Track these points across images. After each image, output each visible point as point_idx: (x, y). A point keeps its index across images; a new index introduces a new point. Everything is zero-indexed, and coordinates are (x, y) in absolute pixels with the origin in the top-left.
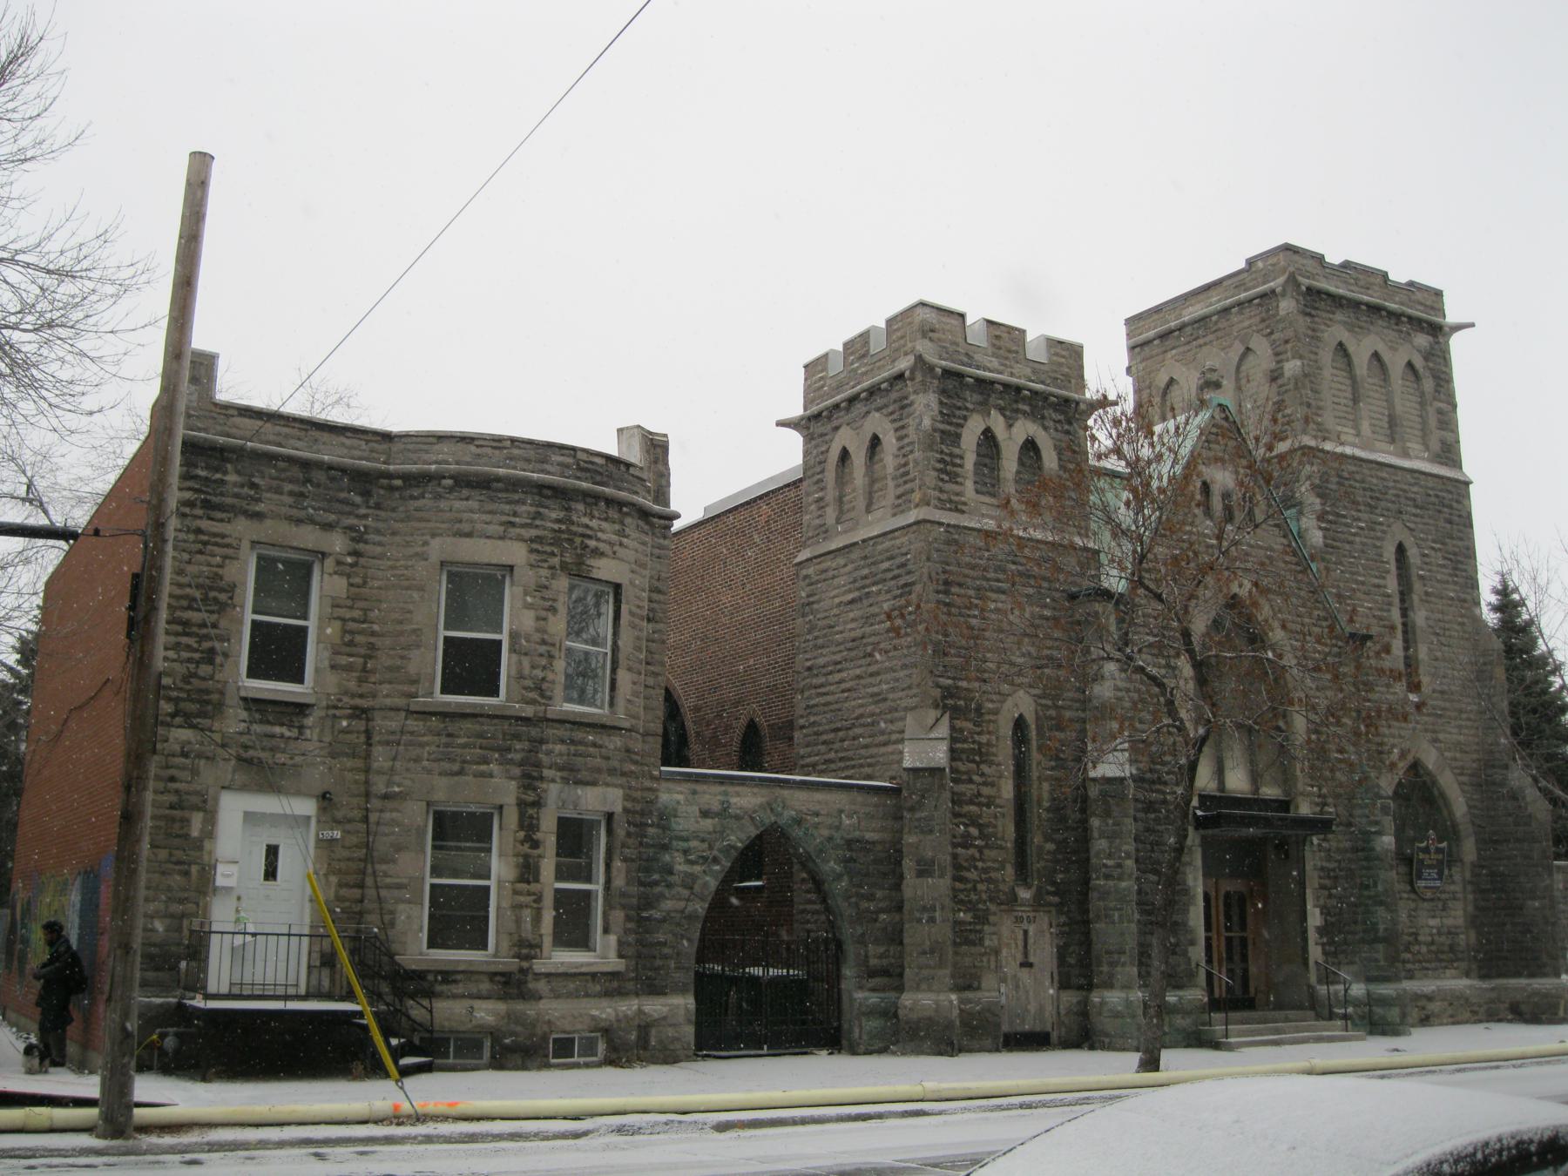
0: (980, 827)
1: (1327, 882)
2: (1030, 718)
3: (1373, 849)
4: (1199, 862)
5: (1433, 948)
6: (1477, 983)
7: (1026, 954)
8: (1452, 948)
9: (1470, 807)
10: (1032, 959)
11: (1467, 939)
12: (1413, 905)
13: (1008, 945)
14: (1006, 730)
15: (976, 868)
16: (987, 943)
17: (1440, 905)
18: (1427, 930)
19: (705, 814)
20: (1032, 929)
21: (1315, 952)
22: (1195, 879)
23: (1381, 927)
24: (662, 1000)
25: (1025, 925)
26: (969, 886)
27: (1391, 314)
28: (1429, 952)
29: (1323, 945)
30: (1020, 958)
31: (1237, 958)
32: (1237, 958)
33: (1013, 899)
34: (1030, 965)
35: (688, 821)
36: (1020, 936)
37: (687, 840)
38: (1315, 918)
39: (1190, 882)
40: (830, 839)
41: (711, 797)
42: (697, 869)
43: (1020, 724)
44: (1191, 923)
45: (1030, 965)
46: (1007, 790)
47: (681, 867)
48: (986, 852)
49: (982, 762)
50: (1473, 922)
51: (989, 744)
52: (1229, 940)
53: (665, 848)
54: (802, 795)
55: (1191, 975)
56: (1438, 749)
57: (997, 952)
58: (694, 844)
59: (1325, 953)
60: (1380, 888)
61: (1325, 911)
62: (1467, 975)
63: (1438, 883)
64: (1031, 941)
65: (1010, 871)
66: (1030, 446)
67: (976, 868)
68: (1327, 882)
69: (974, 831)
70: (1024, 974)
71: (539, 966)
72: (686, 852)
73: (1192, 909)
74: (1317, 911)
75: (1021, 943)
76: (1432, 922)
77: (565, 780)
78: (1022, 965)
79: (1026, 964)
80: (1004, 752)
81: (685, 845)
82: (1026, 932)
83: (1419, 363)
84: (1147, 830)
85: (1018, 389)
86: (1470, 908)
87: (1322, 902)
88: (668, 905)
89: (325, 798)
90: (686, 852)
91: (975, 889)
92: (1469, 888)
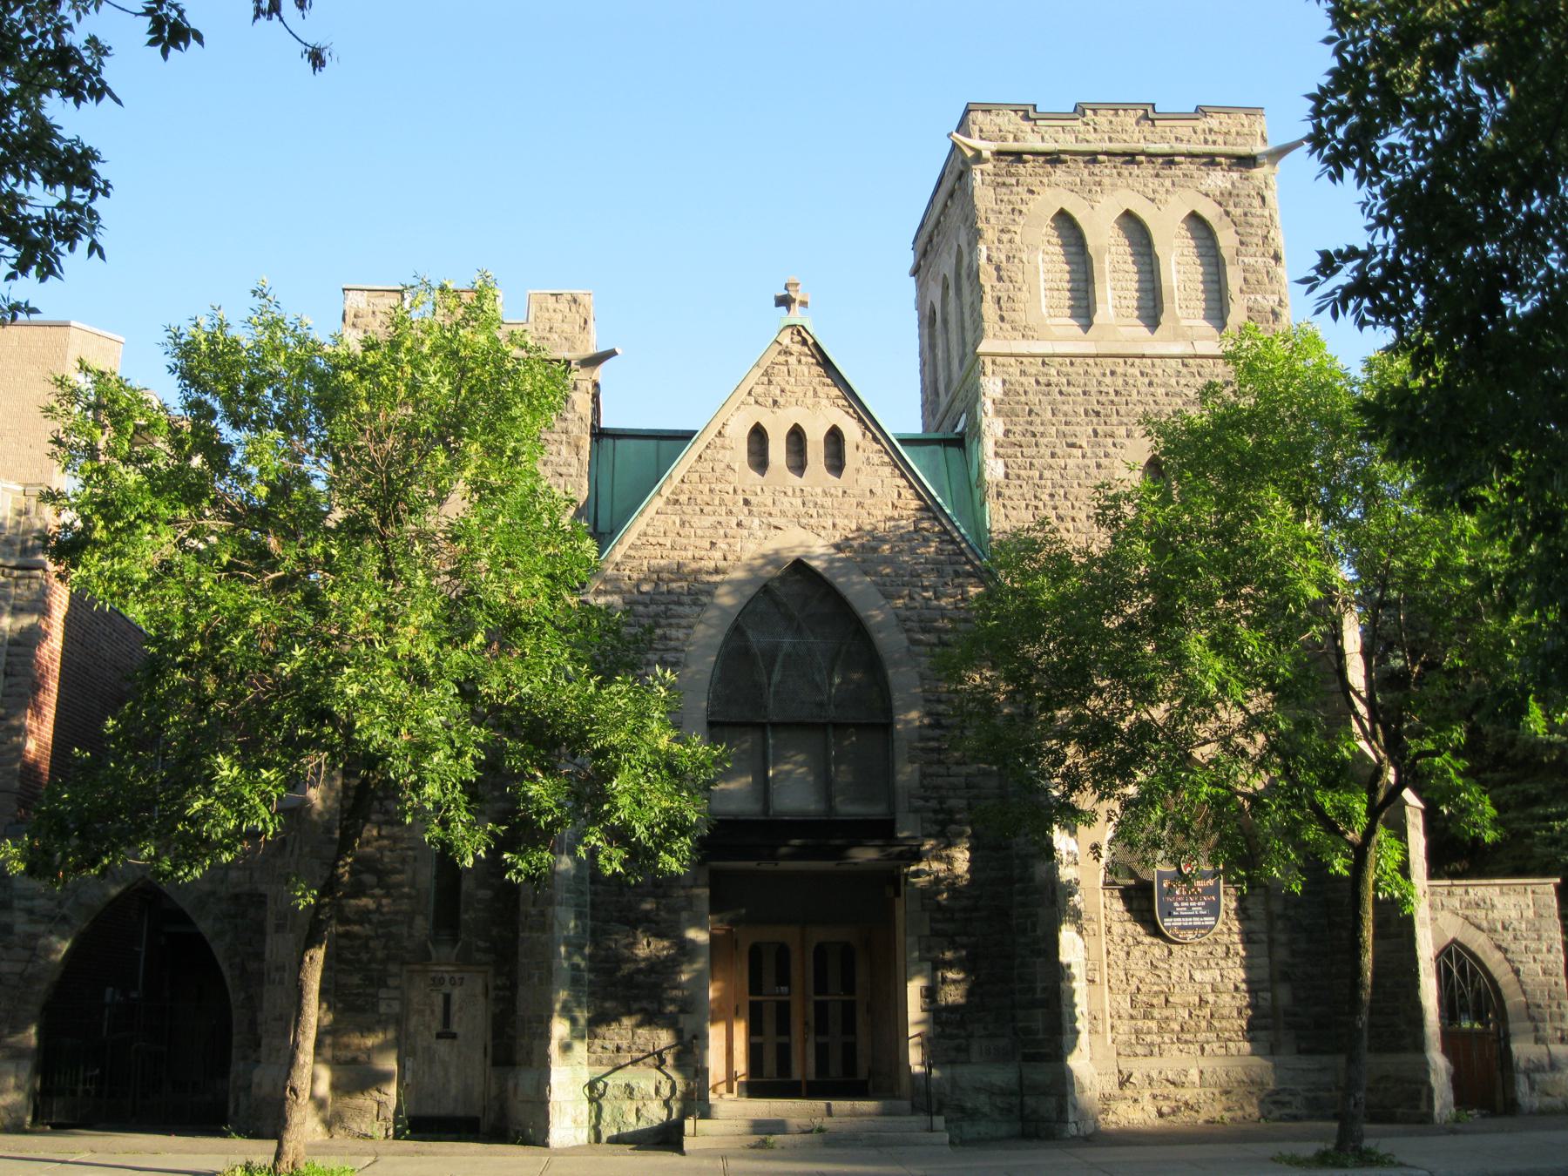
3: (1031, 879)
10: (455, 1028)
13: (421, 1013)
15: (370, 922)
16: (383, 1008)
17: (1220, 951)
20: (457, 994)
23: (1039, 985)
25: (446, 988)
26: (358, 942)
30: (437, 1026)
37: (32, 898)
40: (213, 893)
42: (42, 928)
45: (454, 1036)
49: (386, 798)
52: (821, 1008)
60: (1039, 932)
63: (1209, 921)
64: (454, 1008)
65: (422, 925)
67: (370, 922)
70: (443, 1047)
72: (30, 912)
75: (439, 1010)
78: (439, 1036)
79: (446, 1034)
81: (28, 904)
82: (447, 999)
83: (1209, 211)
86: (1282, 954)
90: (30, 912)
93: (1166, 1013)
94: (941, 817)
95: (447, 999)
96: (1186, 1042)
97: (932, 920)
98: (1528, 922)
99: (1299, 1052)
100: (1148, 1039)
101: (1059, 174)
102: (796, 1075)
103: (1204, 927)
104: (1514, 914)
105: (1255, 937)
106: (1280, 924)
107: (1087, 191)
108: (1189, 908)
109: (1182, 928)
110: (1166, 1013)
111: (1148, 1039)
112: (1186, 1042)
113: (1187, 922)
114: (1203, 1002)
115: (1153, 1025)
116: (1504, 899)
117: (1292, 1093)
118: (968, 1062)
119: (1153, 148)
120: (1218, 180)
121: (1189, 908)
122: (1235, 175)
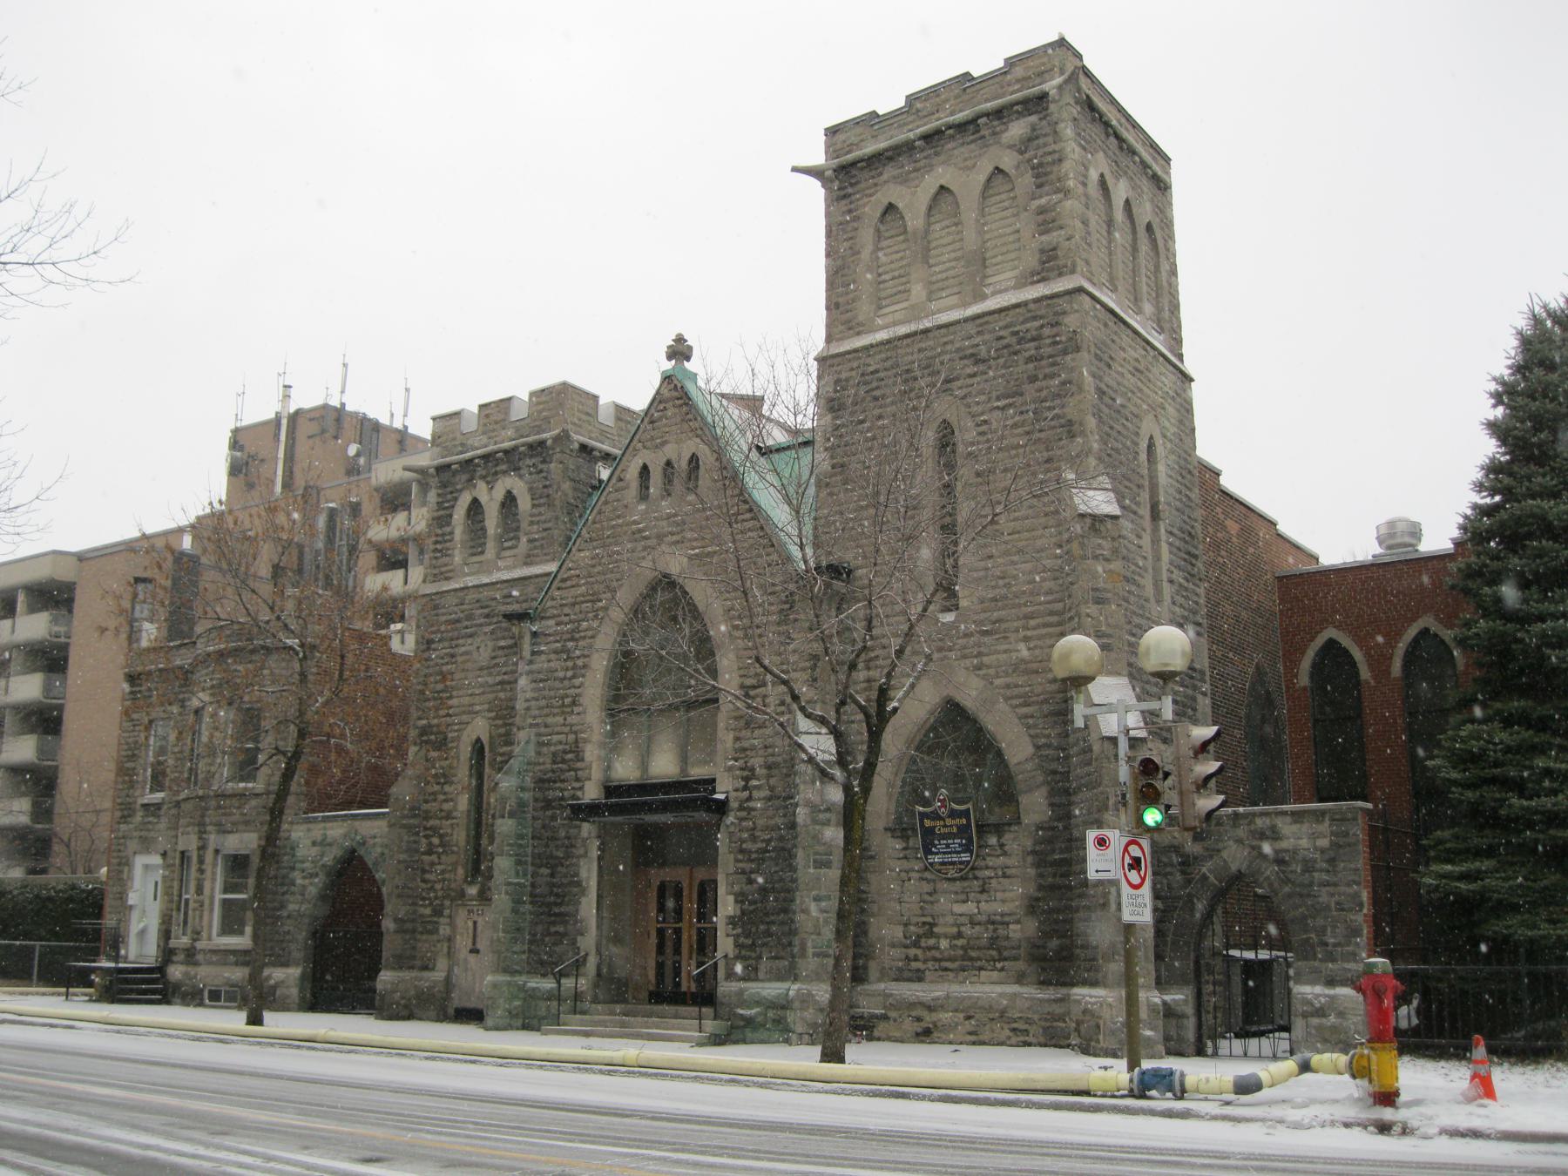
0: (441, 836)
1: (747, 866)
2: (485, 740)
4: (595, 853)
5: (960, 942)
6: (1030, 991)
7: (474, 943)
8: (993, 942)
9: (1038, 747)
10: (479, 946)
11: (1022, 930)
12: (927, 887)
14: (465, 750)
18: (950, 919)
19: (314, 844)
21: (725, 944)
22: (589, 870)
24: (285, 970)
27: (961, 127)
28: (953, 947)
29: (737, 937)
30: (470, 945)
31: (669, 950)
32: (669, 950)
33: (462, 894)
34: (477, 951)
35: (305, 850)
36: (470, 924)
38: (727, 906)
39: (583, 874)
41: (317, 831)
43: (478, 748)
44: (582, 913)
45: (477, 951)
46: (463, 803)
47: (299, 881)
48: (443, 857)
50: (1032, 907)
51: (451, 767)
53: (293, 869)
54: (367, 824)
55: (579, 964)
56: (984, 677)
57: (450, 939)
58: (307, 865)
59: (737, 945)
61: (740, 898)
62: (1020, 979)
63: (965, 857)
64: (479, 928)
66: (510, 500)
68: (747, 866)
69: (436, 841)
70: (472, 958)
71: (199, 945)
73: (583, 900)
74: (731, 898)
76: (958, 908)
77: (219, 832)
80: (463, 773)
82: (475, 923)
84: (544, 827)
85: (515, 449)
87: (736, 888)
88: (291, 907)
89: (164, 855)
91: (432, 888)
92: (1030, 859)
93: (932, 942)
94: (746, 773)
95: (475, 923)
96: (946, 969)
97: (737, 861)
98: (1323, 851)
99: (1044, 983)
100: (914, 965)
101: (889, 171)
102: (684, 988)
103: (961, 863)
104: (1304, 843)
105: (1008, 872)
106: (1030, 859)
107: (903, 180)
108: (948, 846)
109: (943, 864)
110: (932, 942)
111: (914, 965)
112: (946, 969)
113: (948, 858)
114: (960, 935)
115: (919, 952)
116: (1295, 827)
117: (1028, 1021)
118: (756, 979)
119: (960, 117)
120: (1017, 129)
121: (948, 846)
122: (1034, 118)
